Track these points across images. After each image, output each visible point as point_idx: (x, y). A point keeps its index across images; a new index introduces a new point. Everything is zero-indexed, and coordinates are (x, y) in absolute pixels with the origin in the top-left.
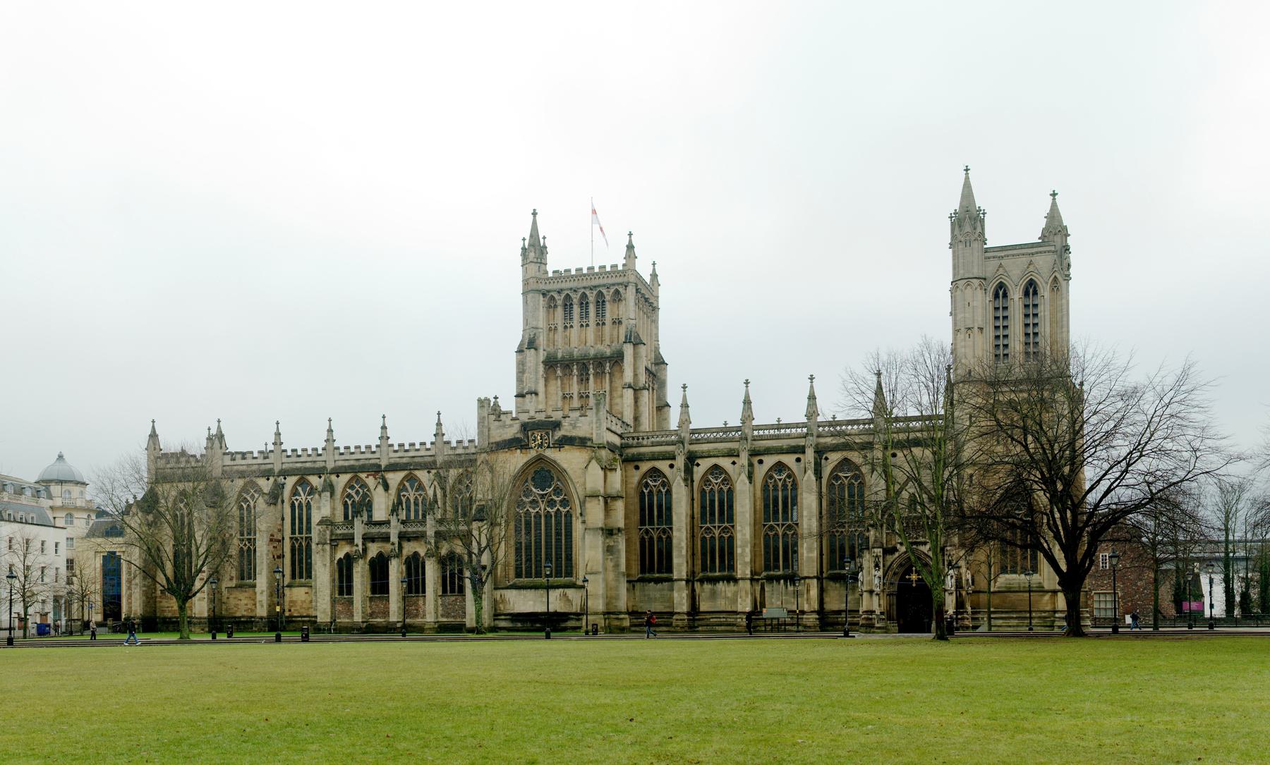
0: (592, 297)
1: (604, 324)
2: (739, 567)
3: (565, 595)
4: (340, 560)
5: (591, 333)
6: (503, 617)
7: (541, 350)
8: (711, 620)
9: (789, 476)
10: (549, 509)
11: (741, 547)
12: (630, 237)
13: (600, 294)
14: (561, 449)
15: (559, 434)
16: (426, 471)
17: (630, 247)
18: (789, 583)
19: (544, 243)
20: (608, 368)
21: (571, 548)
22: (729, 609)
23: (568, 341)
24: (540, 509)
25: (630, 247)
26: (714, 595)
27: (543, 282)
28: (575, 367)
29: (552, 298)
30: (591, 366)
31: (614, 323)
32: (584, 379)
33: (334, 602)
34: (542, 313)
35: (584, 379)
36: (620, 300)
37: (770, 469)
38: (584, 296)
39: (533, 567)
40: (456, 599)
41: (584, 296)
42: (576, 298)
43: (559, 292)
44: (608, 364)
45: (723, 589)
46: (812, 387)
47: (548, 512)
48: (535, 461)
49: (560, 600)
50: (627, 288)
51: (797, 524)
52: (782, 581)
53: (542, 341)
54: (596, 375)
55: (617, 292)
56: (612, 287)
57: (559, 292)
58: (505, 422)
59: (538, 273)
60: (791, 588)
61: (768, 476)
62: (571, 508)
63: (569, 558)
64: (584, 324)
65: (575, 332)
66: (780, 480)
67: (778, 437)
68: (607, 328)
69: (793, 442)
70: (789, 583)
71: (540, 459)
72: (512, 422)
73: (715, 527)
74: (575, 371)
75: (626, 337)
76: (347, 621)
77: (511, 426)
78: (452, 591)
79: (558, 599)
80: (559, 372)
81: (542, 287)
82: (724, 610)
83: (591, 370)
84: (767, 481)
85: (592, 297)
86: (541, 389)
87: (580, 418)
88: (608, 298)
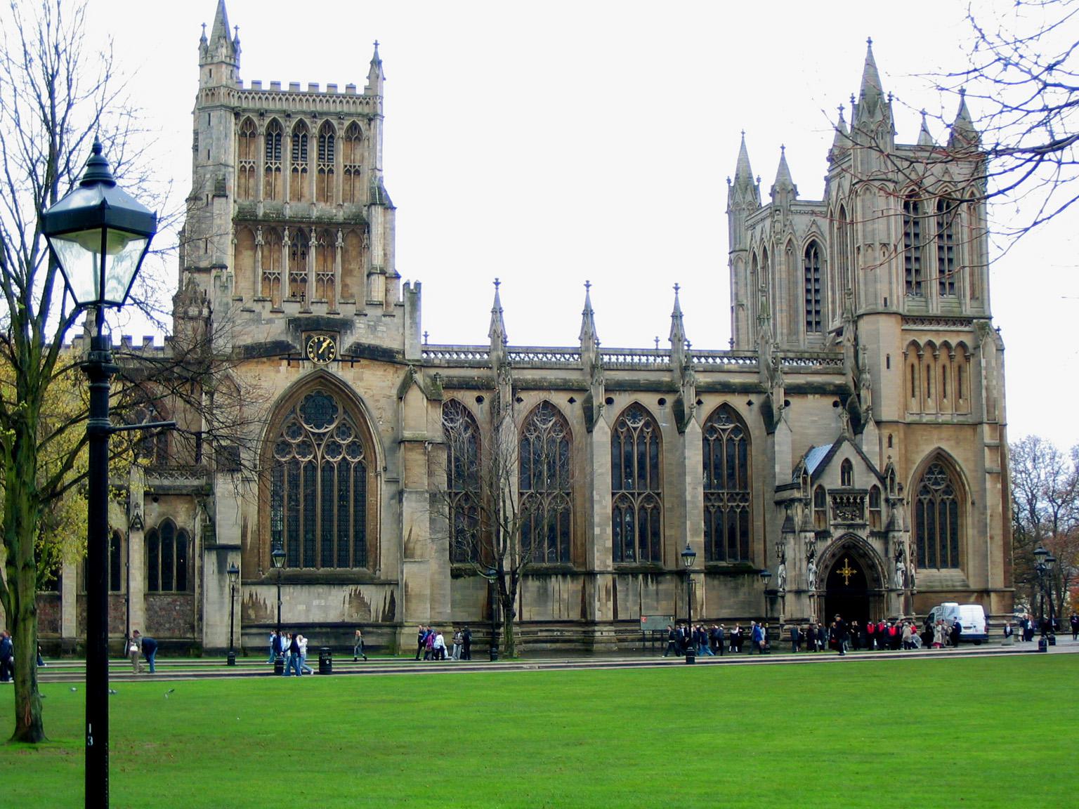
0: (314, 128)
1: (331, 171)
2: (597, 554)
3: (358, 595)
5: (311, 184)
6: (254, 631)
7: (232, 201)
8: (539, 634)
9: (647, 425)
10: (328, 458)
11: (599, 525)
12: (376, 48)
13: (327, 126)
14: (354, 364)
15: (348, 341)
17: (376, 63)
18: (650, 580)
19: (236, 36)
20: (340, 240)
21: (364, 521)
22: (565, 618)
23: (270, 194)
24: (314, 458)
25: (376, 63)
26: (543, 596)
27: (236, 96)
28: (287, 232)
29: (249, 122)
30: (313, 234)
31: (348, 172)
32: (299, 255)
34: (232, 144)
35: (299, 255)
36: (358, 139)
37: (622, 414)
38: (301, 125)
39: (302, 550)
40: (175, 601)
41: (301, 125)
42: (288, 127)
43: (262, 115)
44: (340, 234)
45: (557, 588)
46: (677, 299)
47: (328, 462)
48: (312, 380)
49: (350, 602)
50: (373, 123)
51: (658, 494)
52: (640, 577)
53: (232, 183)
54: (319, 247)
55: (354, 127)
56: (346, 118)
57: (262, 115)
58: (260, 314)
59: (229, 81)
60: (652, 587)
61: (620, 423)
62: (364, 458)
63: (360, 536)
64: (300, 168)
65: (285, 179)
66: (635, 429)
67: (632, 368)
68: (339, 177)
69: (652, 377)
70: (650, 580)
71: (323, 379)
72: (273, 316)
73: (632, 494)
74: (286, 239)
75: (373, 195)
77: (270, 321)
78: (167, 586)
79: (347, 602)
80: (260, 238)
81: (234, 102)
82: (556, 618)
83: (313, 240)
84: (616, 429)
85: (314, 128)
86: (229, 261)
87: (383, 318)
88: (341, 133)
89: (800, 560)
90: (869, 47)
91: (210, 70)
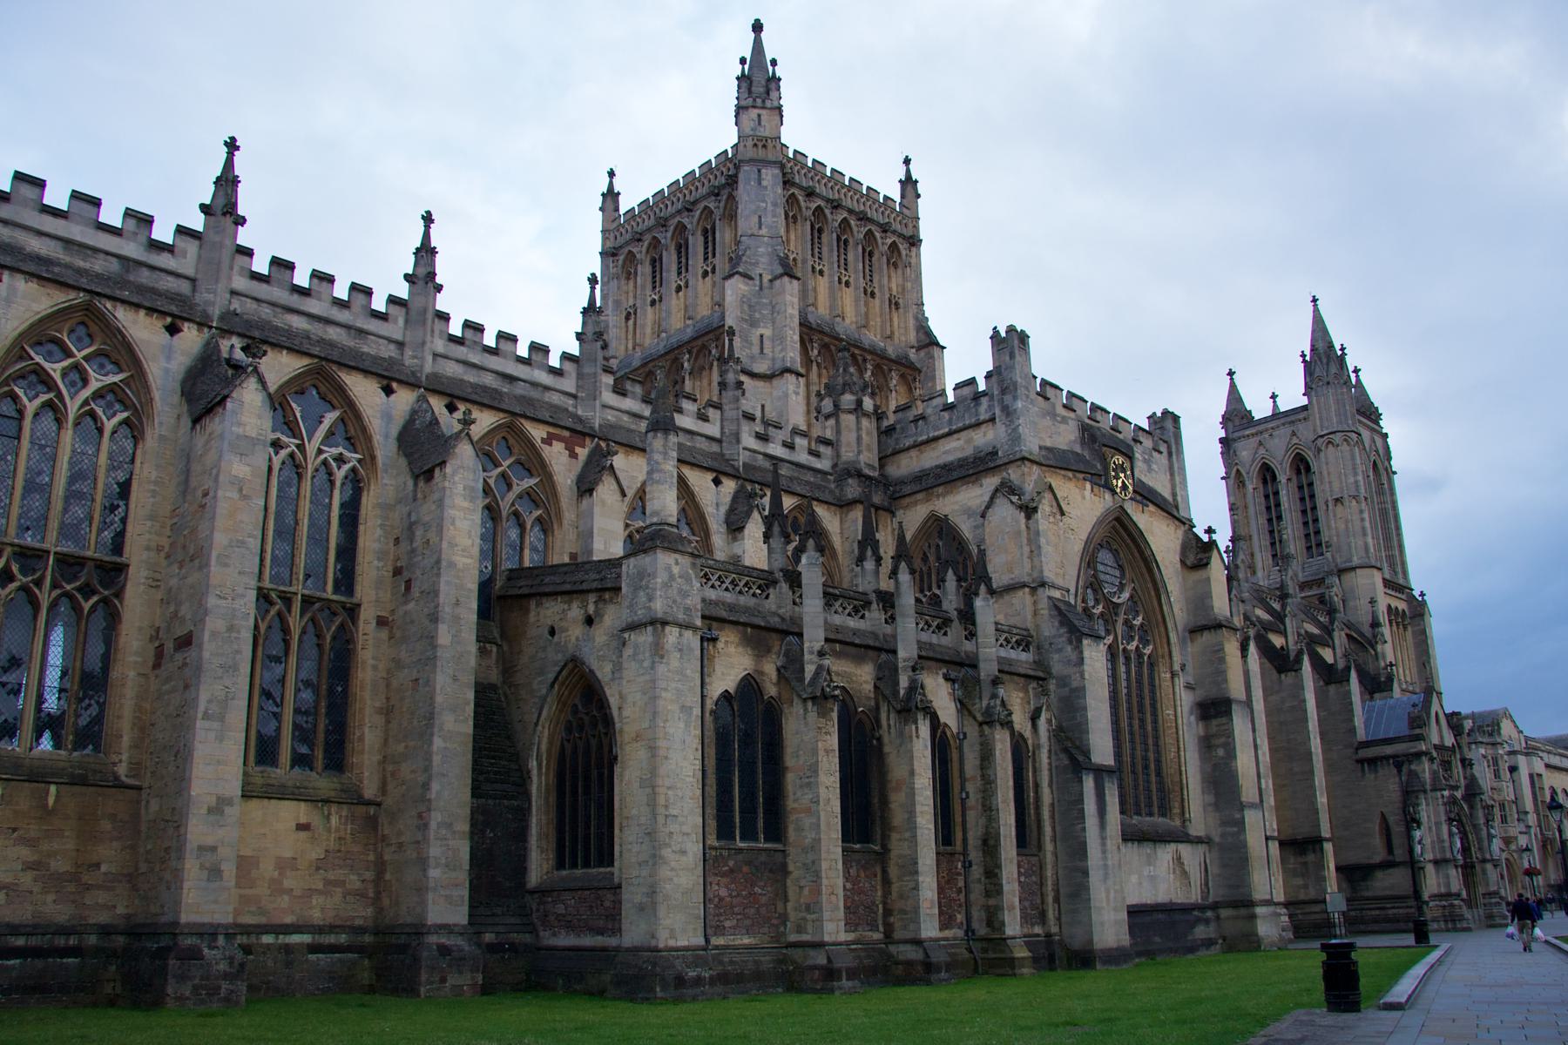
3: (1178, 860)
4: (726, 695)
16: (710, 476)
33: (709, 862)
55: (894, 246)
76: (746, 941)
89: (1438, 824)
90: (1315, 306)
91: (759, 116)
